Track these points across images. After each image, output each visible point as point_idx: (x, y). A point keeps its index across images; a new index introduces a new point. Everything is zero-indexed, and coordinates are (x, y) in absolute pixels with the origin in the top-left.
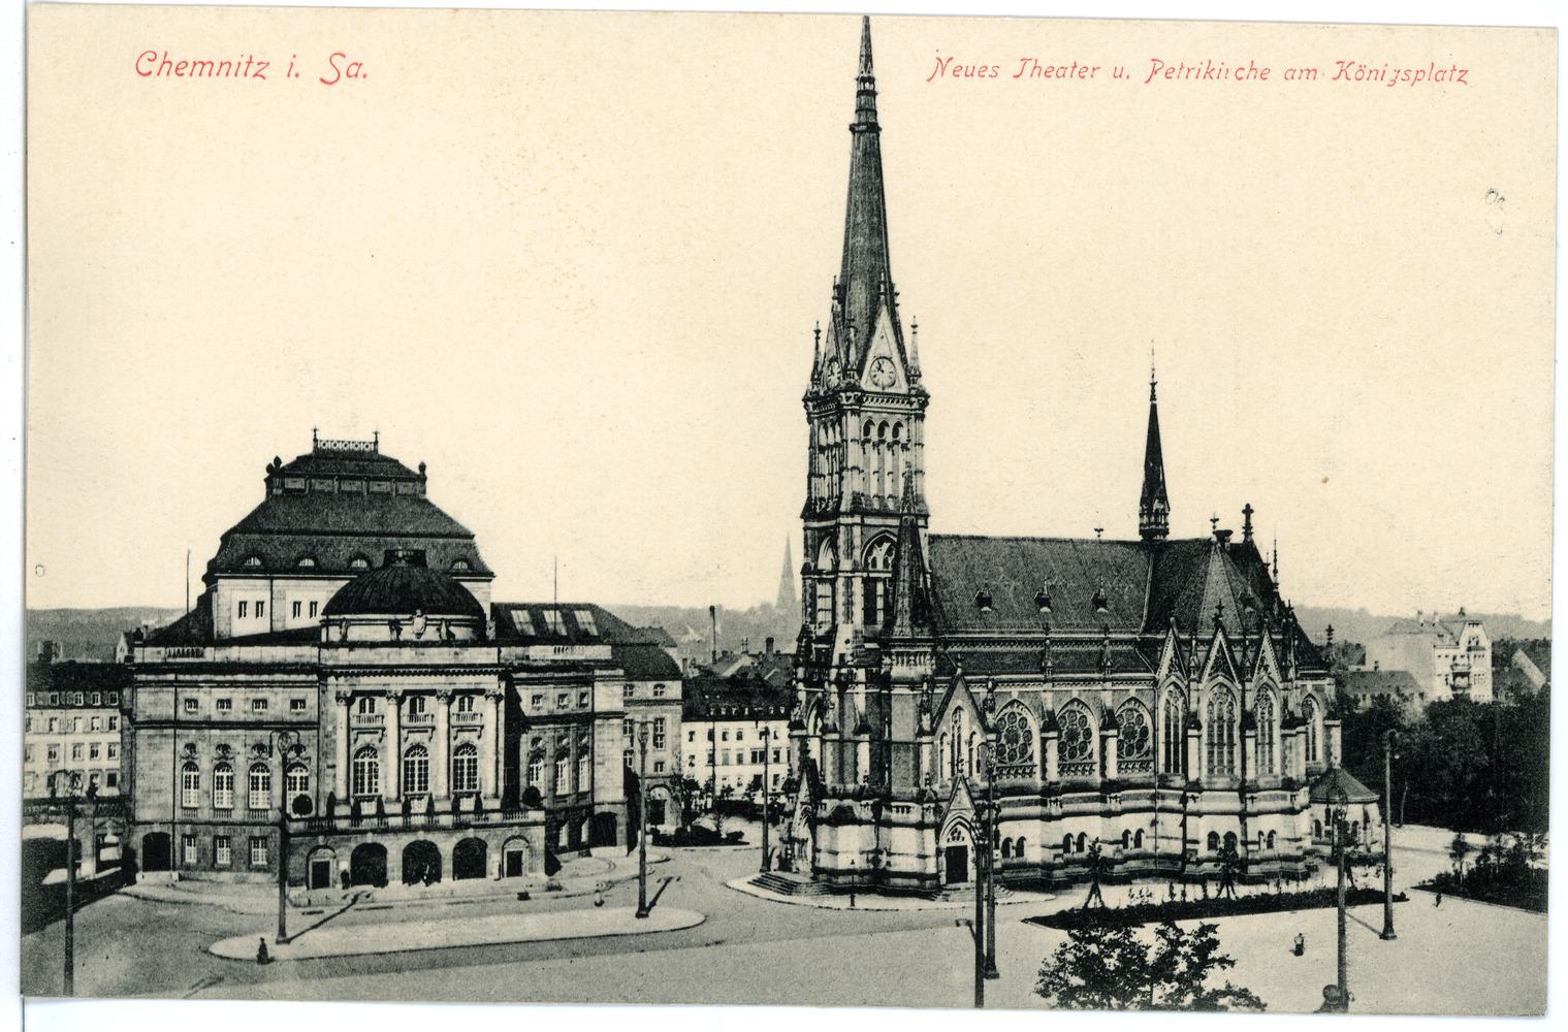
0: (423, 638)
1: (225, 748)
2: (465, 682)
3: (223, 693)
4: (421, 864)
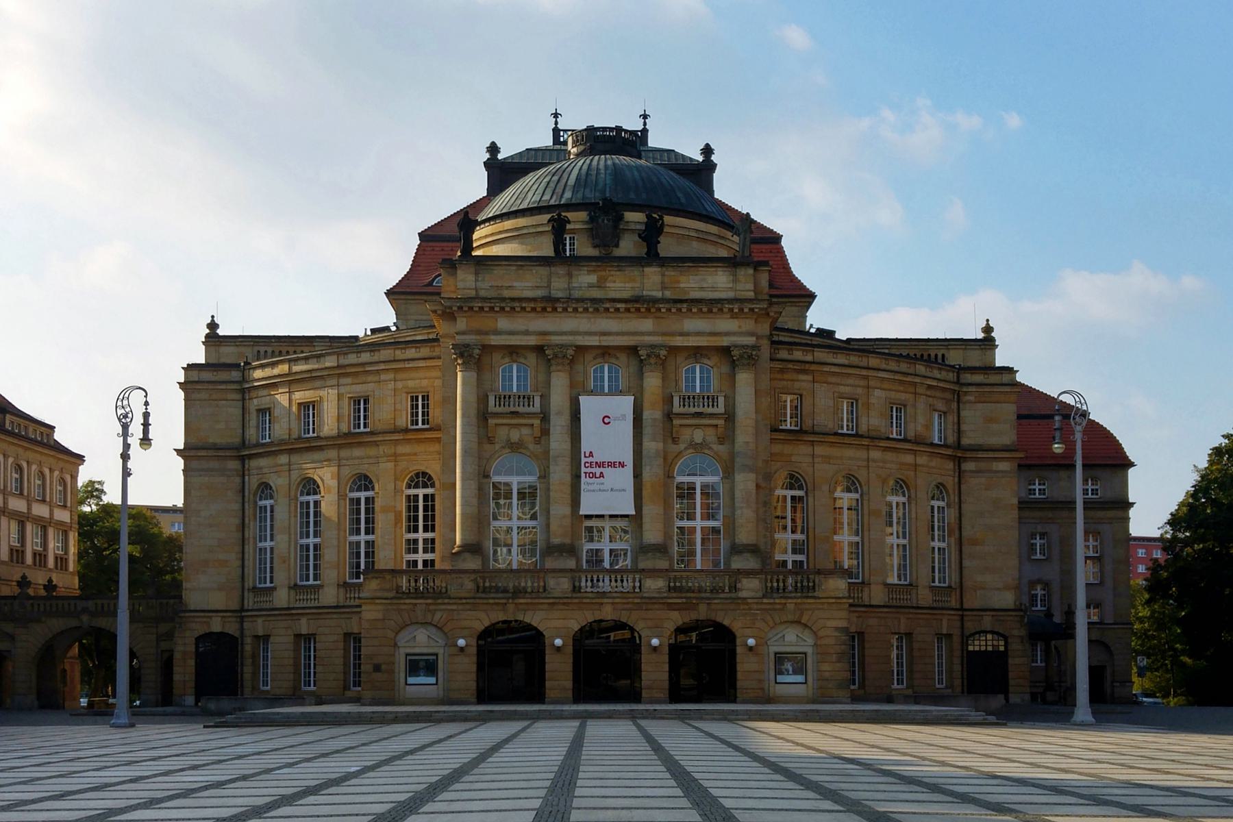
0: (618, 252)
1: (311, 486)
2: (696, 329)
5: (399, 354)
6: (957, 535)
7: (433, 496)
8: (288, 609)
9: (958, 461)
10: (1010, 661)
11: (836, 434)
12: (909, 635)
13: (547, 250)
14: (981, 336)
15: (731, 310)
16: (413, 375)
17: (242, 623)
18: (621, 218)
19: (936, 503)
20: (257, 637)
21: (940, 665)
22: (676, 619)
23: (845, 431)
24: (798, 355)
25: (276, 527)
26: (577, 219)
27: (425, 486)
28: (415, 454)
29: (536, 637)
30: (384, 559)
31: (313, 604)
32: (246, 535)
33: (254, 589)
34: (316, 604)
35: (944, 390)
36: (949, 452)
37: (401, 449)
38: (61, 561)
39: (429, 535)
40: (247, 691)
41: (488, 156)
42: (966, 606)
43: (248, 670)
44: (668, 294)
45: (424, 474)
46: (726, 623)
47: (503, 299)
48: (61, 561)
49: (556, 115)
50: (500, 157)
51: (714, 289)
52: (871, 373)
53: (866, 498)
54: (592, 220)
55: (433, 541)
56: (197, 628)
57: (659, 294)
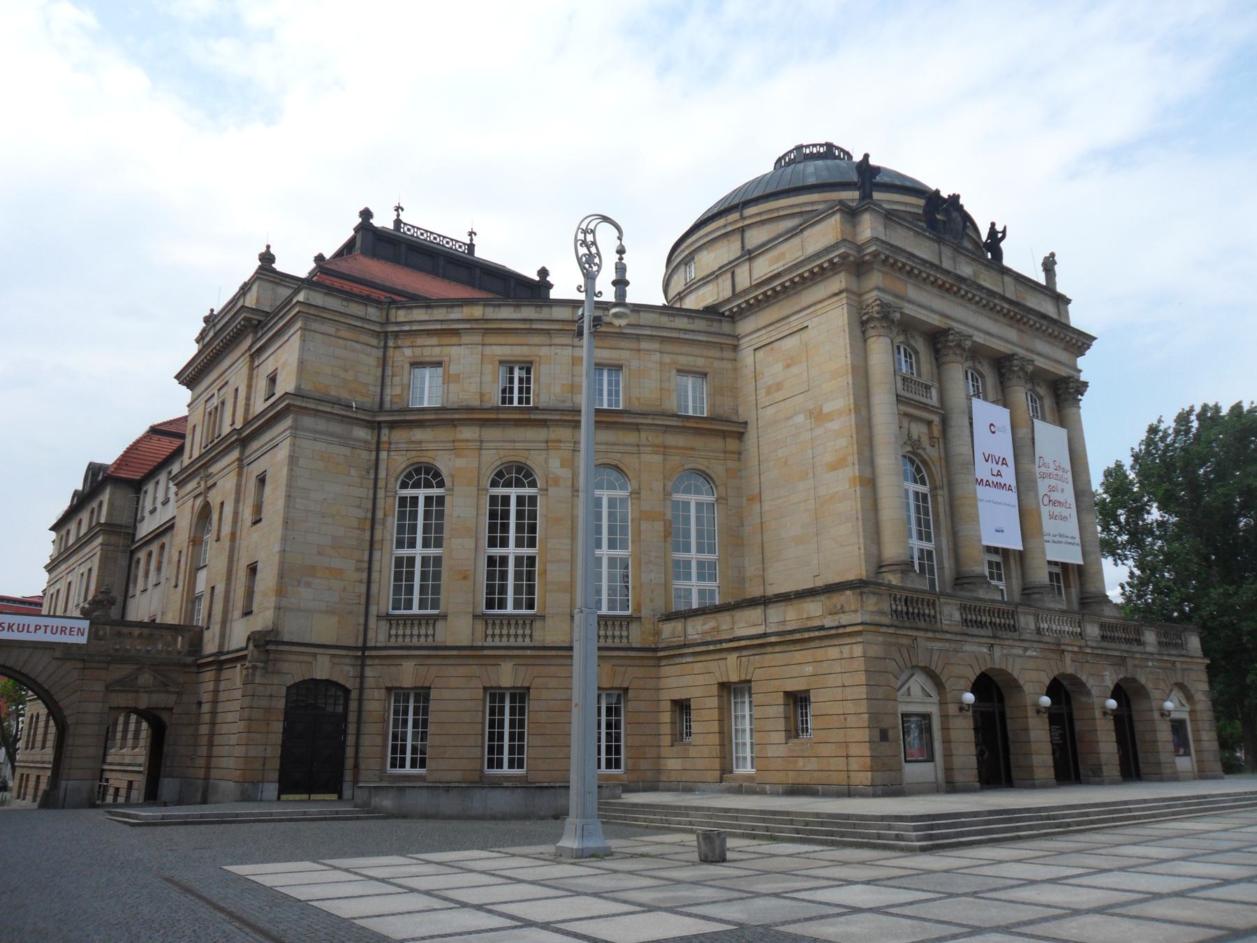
8: (472, 648)
16: (685, 349)
17: (363, 666)
28: (692, 449)
32: (378, 536)
33: (389, 618)
34: (527, 642)
40: (368, 778)
43: (370, 741)
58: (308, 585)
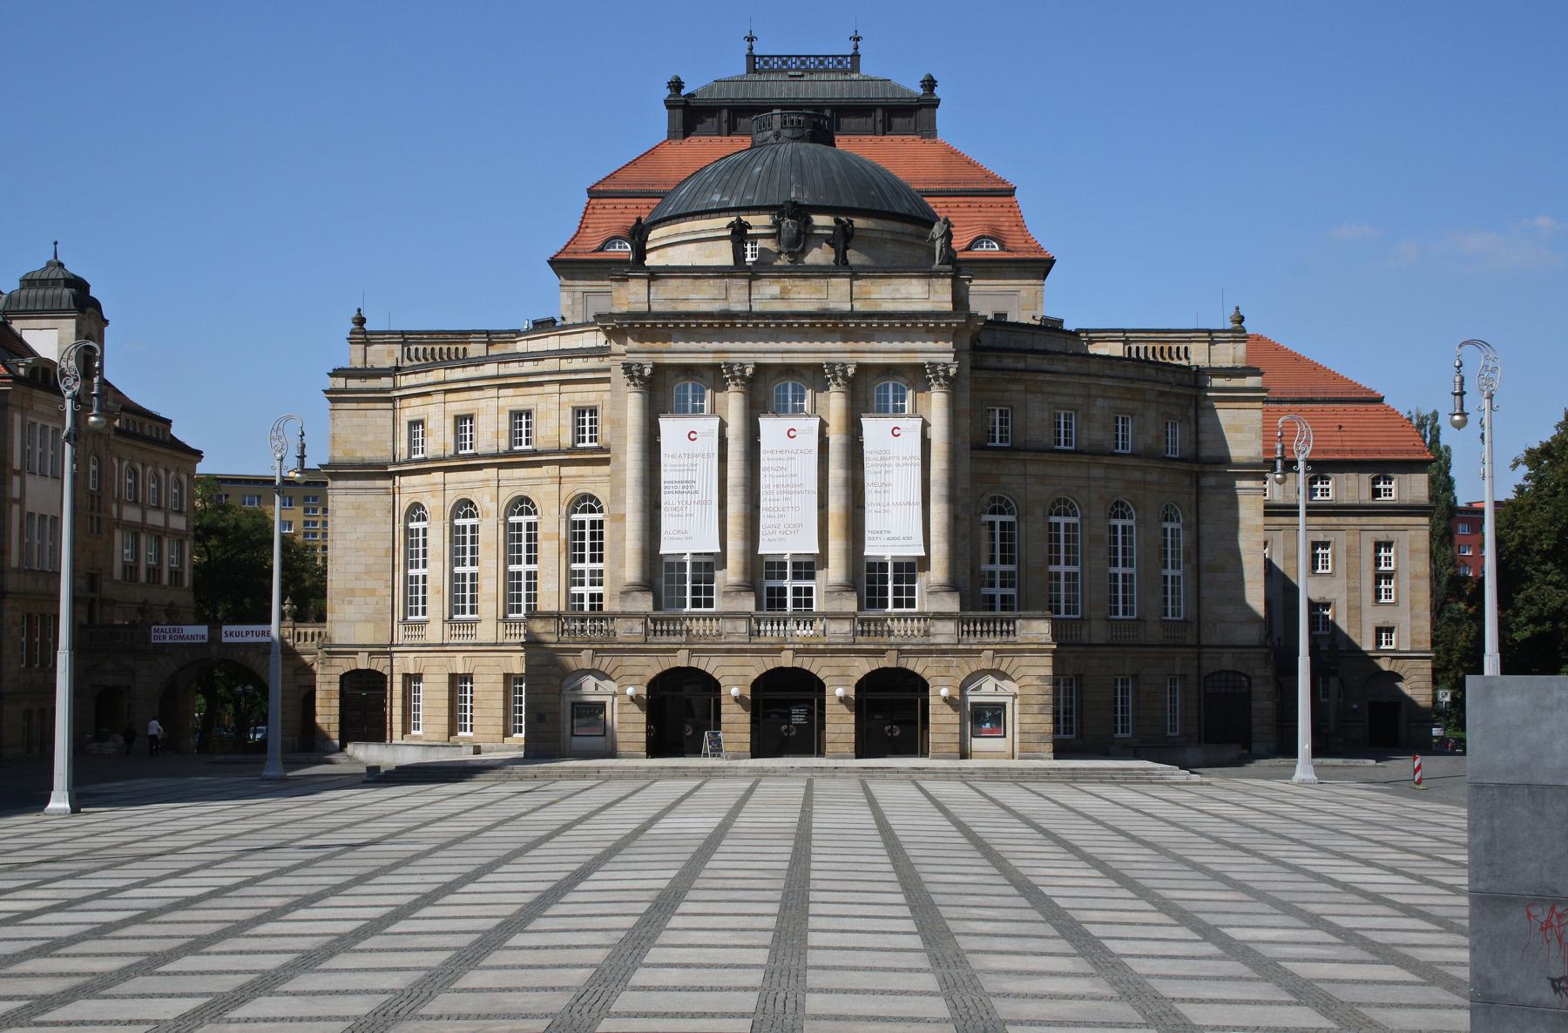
1: (465, 507)
3: (459, 404)
4: (786, 713)
5: (566, 364)
6: (1194, 561)
7: (601, 522)
9: (1198, 476)
10: (1254, 704)
11: (1053, 451)
12: (1135, 676)
13: (722, 255)
14: (1229, 325)
15: (926, 325)
18: (809, 221)
19: (1169, 526)
20: (406, 676)
21: (1173, 709)
22: (863, 667)
23: (1062, 446)
24: (1008, 362)
25: (429, 553)
26: (759, 222)
27: (592, 510)
29: (711, 685)
30: (550, 597)
31: (469, 640)
34: (473, 641)
35: (1177, 395)
36: (1185, 466)
37: (566, 470)
38: (176, 575)
39: (597, 566)
41: (668, 92)
42: (1204, 642)
44: (858, 307)
45: (592, 497)
46: (918, 670)
47: (678, 315)
48: (176, 575)
49: (751, 39)
50: (684, 92)
51: (908, 299)
52: (1095, 381)
53: (1086, 522)
54: (777, 224)
55: (601, 572)
56: (343, 665)
57: (847, 307)
58: (350, 602)
